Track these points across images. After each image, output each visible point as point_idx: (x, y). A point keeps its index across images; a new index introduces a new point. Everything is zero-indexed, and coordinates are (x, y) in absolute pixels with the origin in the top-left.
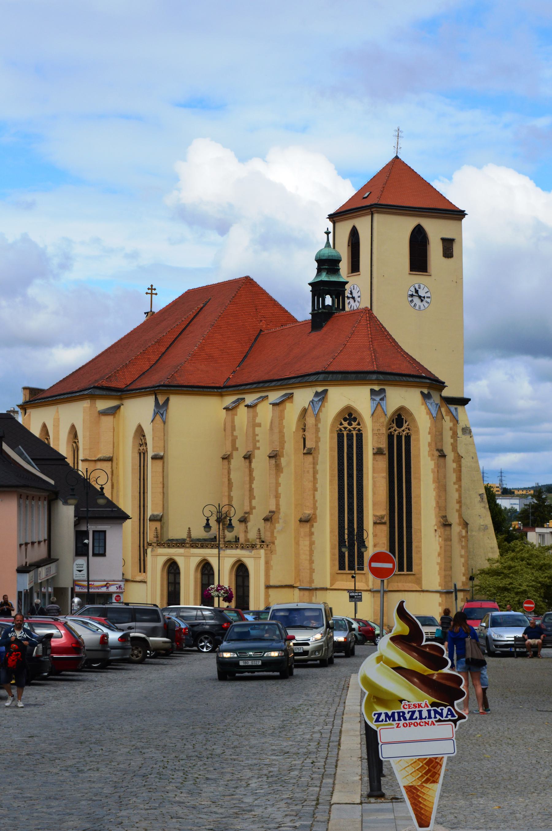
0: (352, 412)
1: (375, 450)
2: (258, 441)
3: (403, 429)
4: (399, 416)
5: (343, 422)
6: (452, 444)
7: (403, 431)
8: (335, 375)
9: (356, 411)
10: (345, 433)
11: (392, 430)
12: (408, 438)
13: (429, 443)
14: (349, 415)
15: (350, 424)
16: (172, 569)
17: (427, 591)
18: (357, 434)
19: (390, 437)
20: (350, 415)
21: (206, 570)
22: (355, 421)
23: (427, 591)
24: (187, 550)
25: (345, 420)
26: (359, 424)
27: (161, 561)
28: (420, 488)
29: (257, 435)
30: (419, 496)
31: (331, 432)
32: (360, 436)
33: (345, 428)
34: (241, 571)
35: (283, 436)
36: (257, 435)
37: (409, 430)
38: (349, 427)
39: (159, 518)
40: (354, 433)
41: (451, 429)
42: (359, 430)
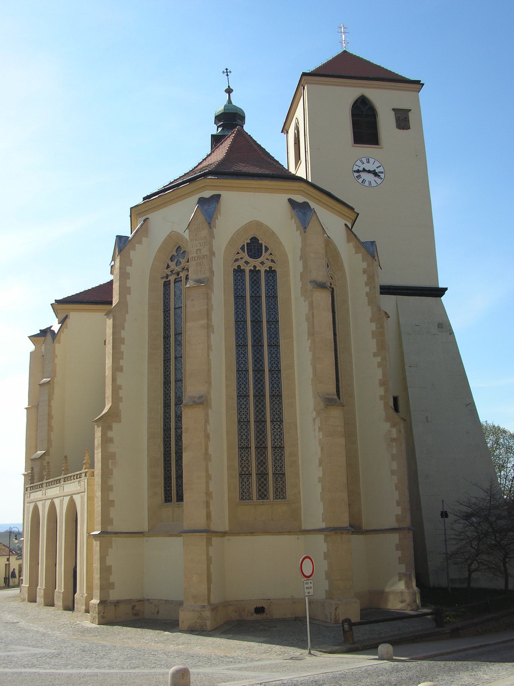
3: (260, 260)
6: (367, 294)
7: (262, 263)
12: (271, 273)
13: (301, 274)
19: (238, 272)
37: (272, 261)
41: (364, 272)
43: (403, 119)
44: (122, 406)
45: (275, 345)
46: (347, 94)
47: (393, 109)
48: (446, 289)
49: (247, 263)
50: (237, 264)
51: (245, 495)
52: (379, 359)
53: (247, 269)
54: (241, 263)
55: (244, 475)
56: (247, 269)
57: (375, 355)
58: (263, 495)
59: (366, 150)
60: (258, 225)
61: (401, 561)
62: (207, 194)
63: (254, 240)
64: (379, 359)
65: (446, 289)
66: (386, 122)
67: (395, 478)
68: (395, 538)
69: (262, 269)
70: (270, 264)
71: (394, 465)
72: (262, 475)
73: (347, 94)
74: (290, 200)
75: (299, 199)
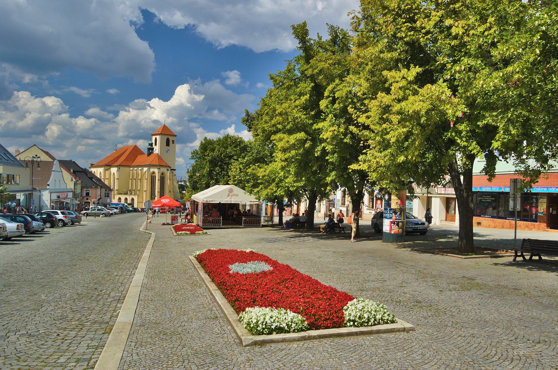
14: (154, 173)
21: (126, 199)
34: (133, 199)
43: (173, 142)
46: (166, 137)
59: (168, 147)
73: (166, 137)
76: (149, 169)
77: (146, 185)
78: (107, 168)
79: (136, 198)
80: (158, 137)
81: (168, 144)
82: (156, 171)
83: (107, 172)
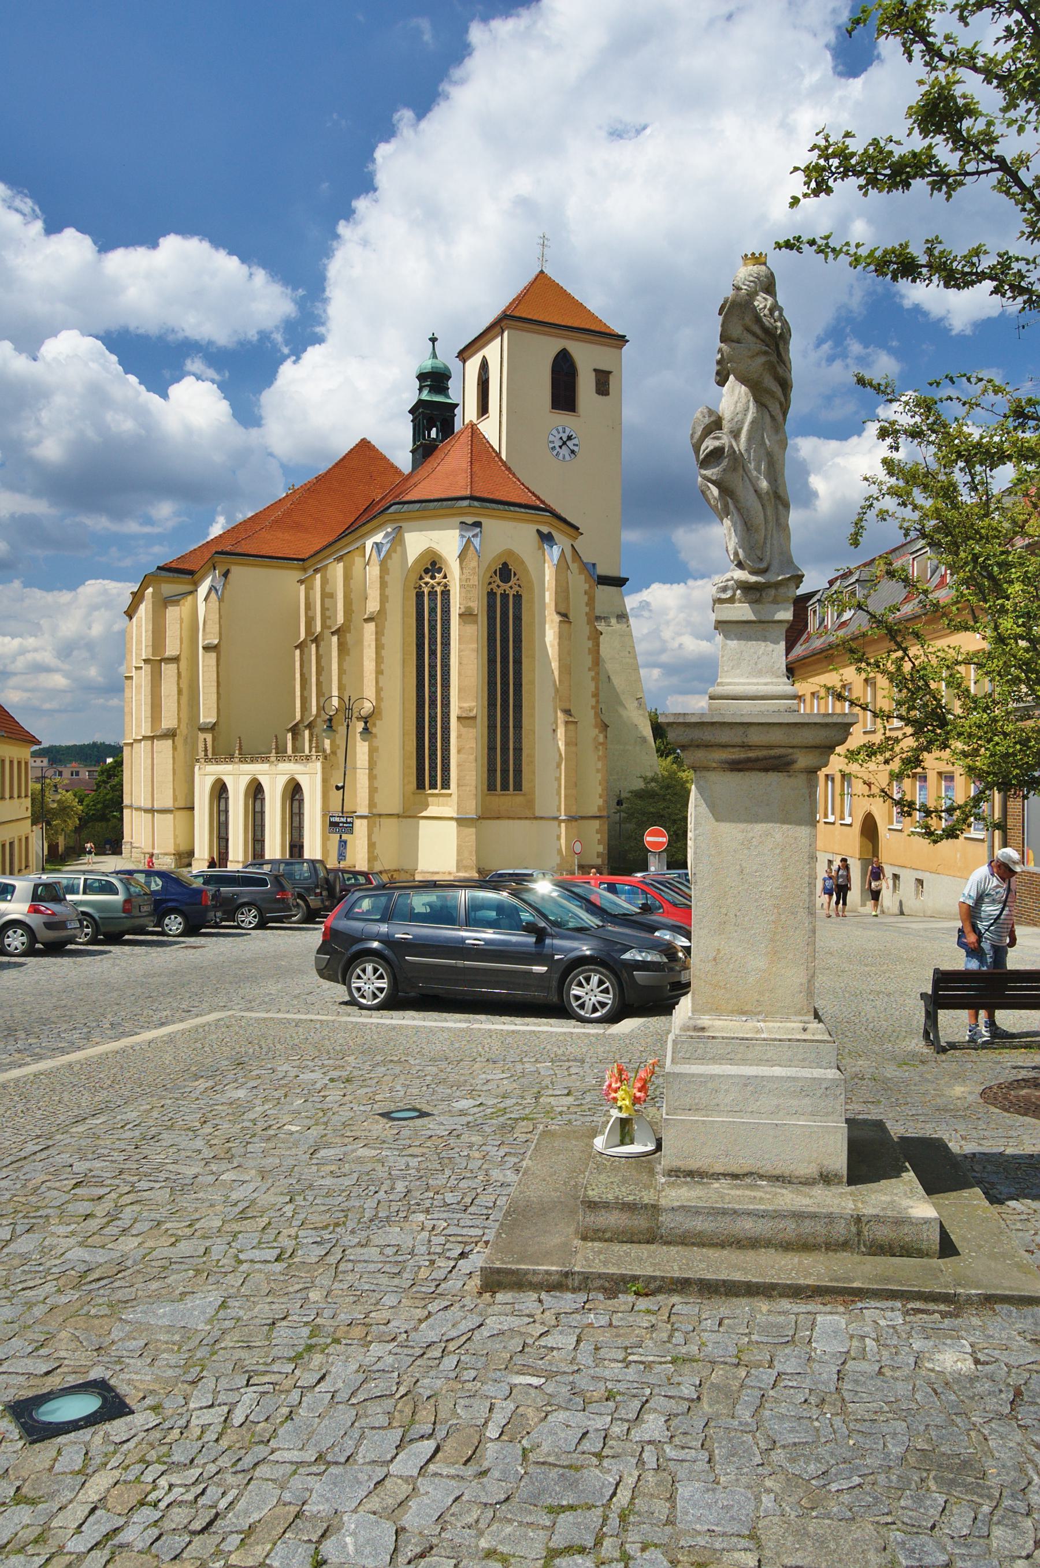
0: (436, 559)
1: (463, 610)
2: (329, 618)
3: (510, 584)
4: (505, 564)
5: (424, 575)
6: (587, 614)
7: (511, 587)
8: (411, 506)
9: (440, 557)
10: (426, 590)
11: (494, 586)
12: (518, 597)
14: (433, 565)
15: (433, 577)
16: (220, 791)
17: (541, 818)
18: (442, 592)
19: (491, 595)
20: (434, 564)
21: (256, 791)
22: (439, 573)
23: (541, 818)
24: (236, 766)
25: (426, 571)
26: (445, 577)
27: (209, 781)
28: (534, 670)
29: (328, 609)
30: (533, 683)
31: (405, 590)
32: (446, 593)
33: (426, 583)
34: (294, 792)
35: (351, 604)
36: (328, 609)
38: (432, 582)
39: (210, 726)
40: (439, 589)
41: (586, 593)
42: (446, 586)
43: (603, 382)
44: (383, 705)
45: (518, 662)
46: (550, 346)
47: (595, 370)
48: (628, 579)
49: (498, 586)
50: (491, 586)
51: (491, 787)
52: (593, 673)
53: (499, 592)
54: (494, 586)
55: (491, 771)
56: (499, 592)
57: (590, 669)
58: (505, 787)
59: (563, 419)
60: (510, 553)
61: (599, 842)
62: (470, 520)
63: (505, 564)
64: (593, 673)
65: (628, 579)
66: (586, 383)
67: (599, 776)
68: (596, 824)
69: (511, 593)
70: (518, 589)
71: (600, 765)
72: (505, 771)
73: (550, 346)
74: (538, 531)
75: (545, 530)
76: (397, 540)
77: (377, 674)
78: (169, 589)
79: (311, 778)
80: (493, 351)
81: (564, 396)
82: (446, 541)
83: (172, 613)
